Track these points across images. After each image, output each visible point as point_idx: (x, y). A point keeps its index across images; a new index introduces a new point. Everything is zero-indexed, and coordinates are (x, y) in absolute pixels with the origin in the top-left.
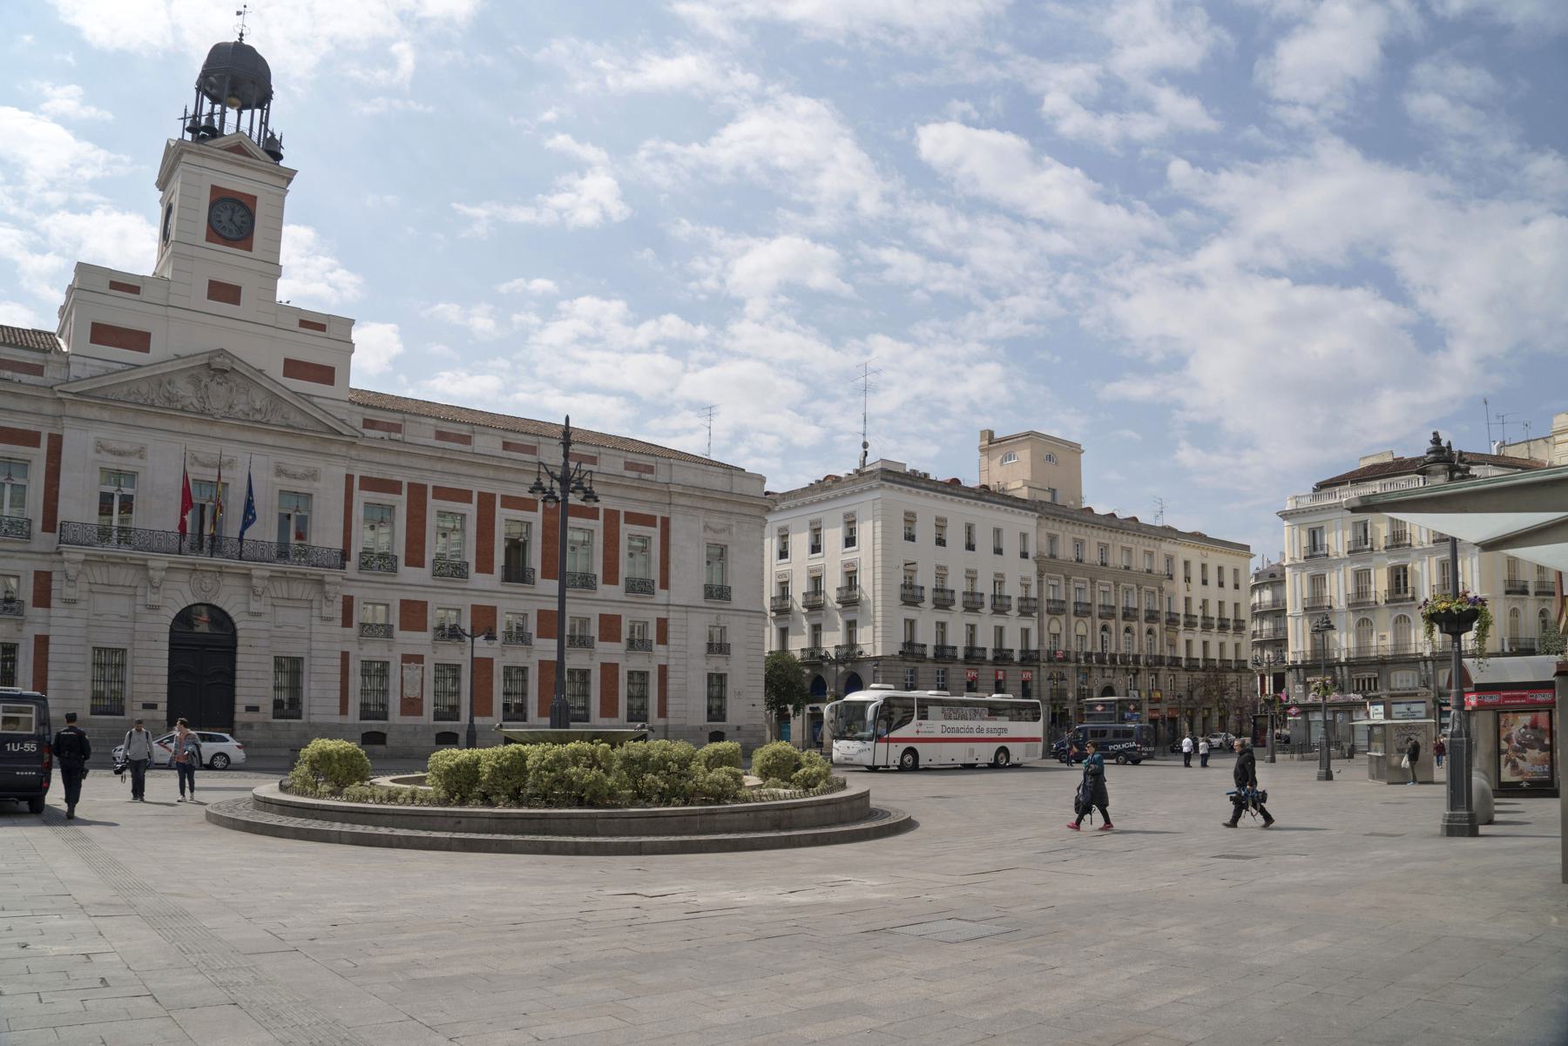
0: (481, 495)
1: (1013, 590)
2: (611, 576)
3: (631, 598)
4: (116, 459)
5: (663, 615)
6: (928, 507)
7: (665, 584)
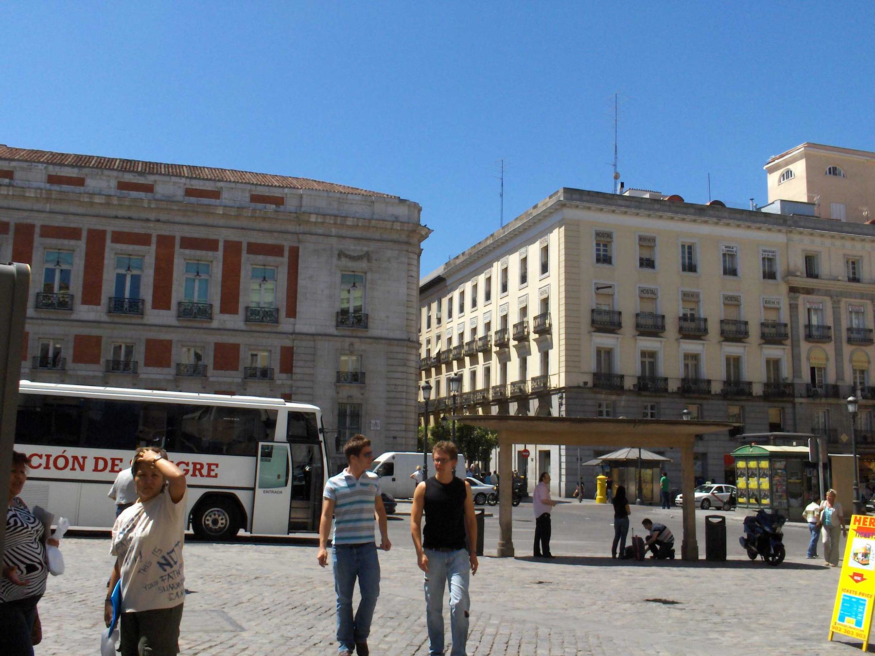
0: (91, 232)
1: (753, 315)
5: (288, 343)
6: (626, 226)
7: (292, 312)
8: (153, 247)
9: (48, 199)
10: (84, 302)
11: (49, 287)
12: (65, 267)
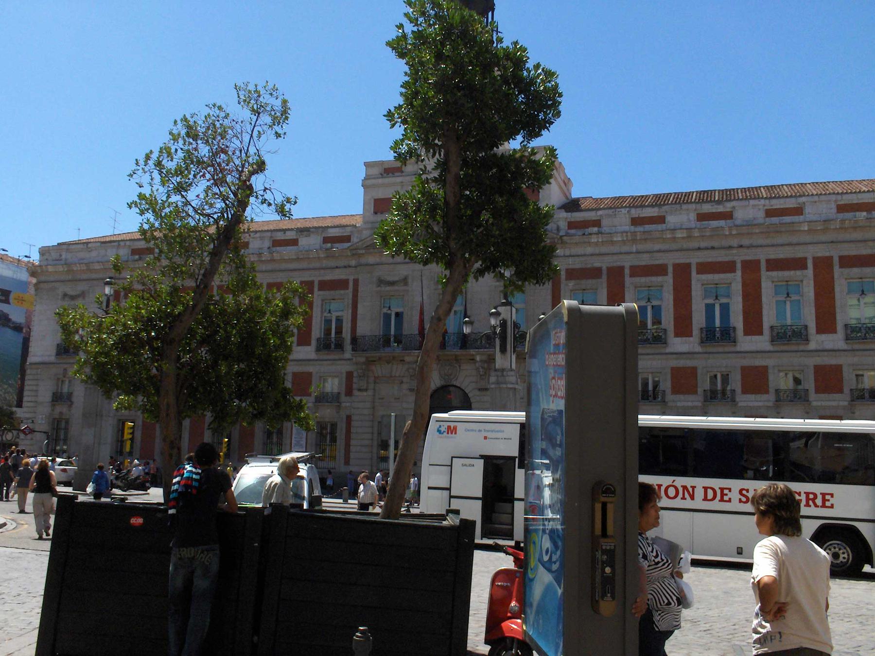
2: (753, 326)
3: (324, 355)
4: (388, 288)
8: (739, 273)
9: (634, 241)
10: (677, 335)
11: (328, 332)
12: (655, 303)
